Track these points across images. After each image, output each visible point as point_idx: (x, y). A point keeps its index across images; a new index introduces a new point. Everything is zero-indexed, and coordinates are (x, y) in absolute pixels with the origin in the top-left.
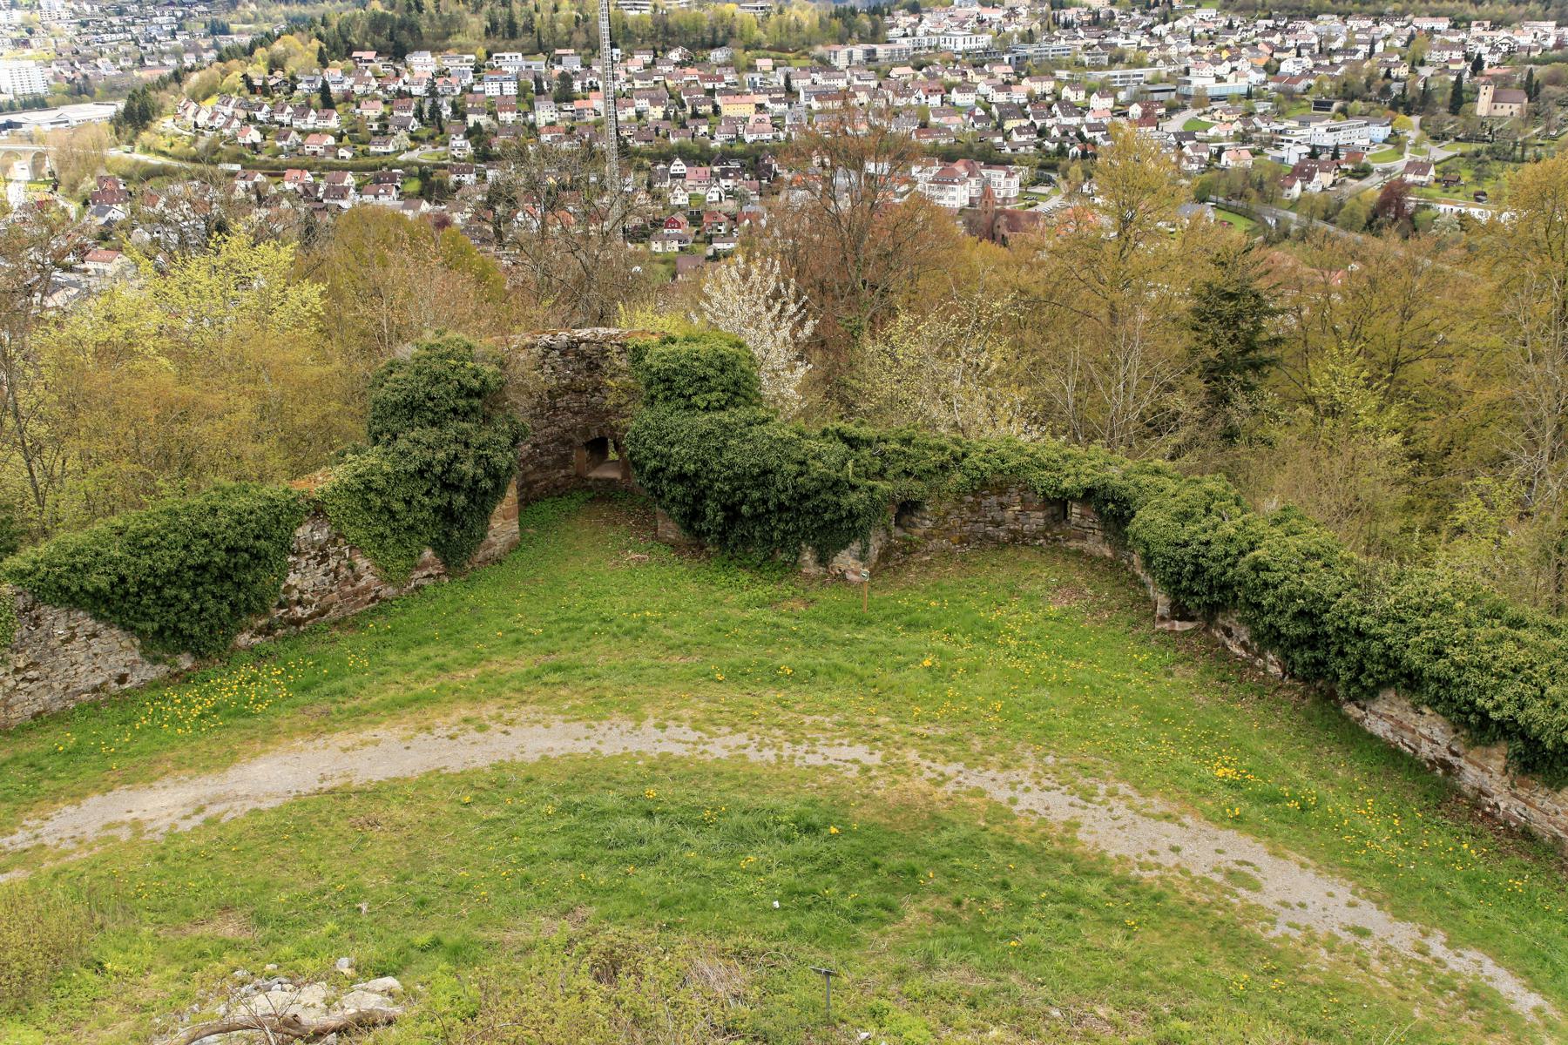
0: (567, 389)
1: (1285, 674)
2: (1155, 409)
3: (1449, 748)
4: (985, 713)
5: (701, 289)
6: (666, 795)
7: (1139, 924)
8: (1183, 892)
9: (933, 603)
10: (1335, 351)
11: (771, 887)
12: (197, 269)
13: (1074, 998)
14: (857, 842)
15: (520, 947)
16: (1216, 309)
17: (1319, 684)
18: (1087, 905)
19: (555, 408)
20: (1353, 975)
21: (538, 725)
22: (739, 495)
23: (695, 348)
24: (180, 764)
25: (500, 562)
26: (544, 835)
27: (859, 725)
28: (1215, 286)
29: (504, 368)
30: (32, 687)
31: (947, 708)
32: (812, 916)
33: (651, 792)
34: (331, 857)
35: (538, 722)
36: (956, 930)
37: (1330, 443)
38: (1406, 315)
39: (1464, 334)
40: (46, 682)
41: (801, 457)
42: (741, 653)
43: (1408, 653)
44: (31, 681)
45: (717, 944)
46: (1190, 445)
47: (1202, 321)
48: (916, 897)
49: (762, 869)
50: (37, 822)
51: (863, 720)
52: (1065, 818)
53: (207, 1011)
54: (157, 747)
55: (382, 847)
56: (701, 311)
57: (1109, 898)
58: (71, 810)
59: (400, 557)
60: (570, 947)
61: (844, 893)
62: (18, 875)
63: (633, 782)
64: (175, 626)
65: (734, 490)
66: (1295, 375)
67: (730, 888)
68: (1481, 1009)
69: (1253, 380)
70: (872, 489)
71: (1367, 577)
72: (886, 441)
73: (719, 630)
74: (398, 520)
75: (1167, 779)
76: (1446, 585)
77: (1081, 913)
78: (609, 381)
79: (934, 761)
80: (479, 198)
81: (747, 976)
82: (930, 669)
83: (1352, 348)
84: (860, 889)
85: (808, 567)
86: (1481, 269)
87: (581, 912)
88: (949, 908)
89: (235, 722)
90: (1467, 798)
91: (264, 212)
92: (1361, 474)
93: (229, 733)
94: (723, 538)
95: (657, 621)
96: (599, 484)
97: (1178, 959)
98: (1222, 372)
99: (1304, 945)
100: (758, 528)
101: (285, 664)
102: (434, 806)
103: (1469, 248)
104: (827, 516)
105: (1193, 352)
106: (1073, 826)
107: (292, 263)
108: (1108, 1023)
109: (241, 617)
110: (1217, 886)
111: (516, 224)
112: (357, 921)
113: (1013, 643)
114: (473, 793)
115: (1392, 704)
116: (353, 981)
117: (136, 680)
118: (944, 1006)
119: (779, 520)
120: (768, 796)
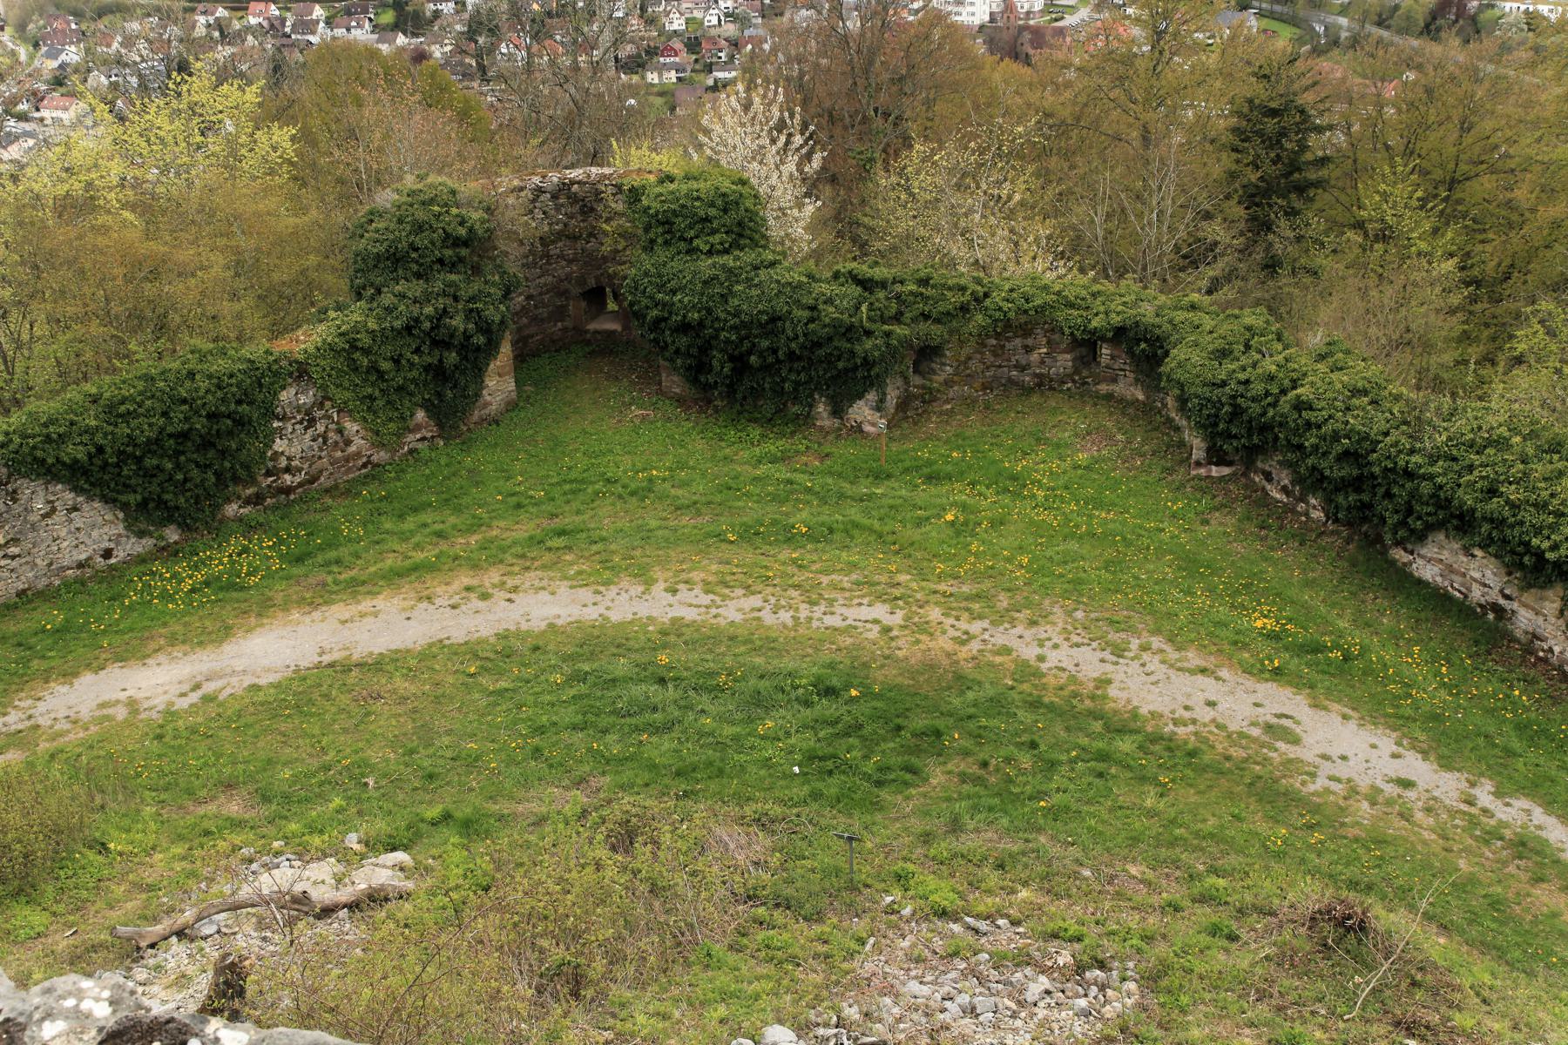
0: (560, 235)
1: (1328, 518)
2: (1191, 240)
3: (1501, 591)
4: (1010, 567)
5: (699, 122)
6: (679, 661)
7: (1173, 781)
8: (1219, 747)
9: (955, 454)
10: (1387, 170)
11: (791, 752)
12: (158, 116)
13: (1106, 858)
14: (879, 704)
15: (532, 819)
16: (1258, 126)
17: (1365, 528)
18: (1119, 763)
19: (548, 256)
20: (1396, 827)
21: (542, 593)
22: (746, 345)
23: (695, 186)
24: (173, 640)
25: (497, 423)
26: (553, 705)
27: (879, 584)
28: (1257, 102)
29: (492, 214)
30: (14, 564)
31: (970, 564)
32: (836, 780)
33: (663, 658)
34: (334, 732)
35: (543, 588)
36: (982, 792)
37: (1380, 270)
38: (1465, 127)
39: (1529, 146)
40: (28, 559)
41: (811, 302)
42: (752, 511)
43: (1460, 492)
44: (13, 558)
45: (734, 810)
46: (1229, 277)
47: (1243, 141)
48: (941, 759)
49: (781, 734)
50: (30, 702)
51: (884, 579)
52: (1095, 675)
53: (215, 889)
54: (149, 623)
55: (387, 720)
56: (699, 147)
57: (1141, 755)
58: (64, 689)
59: (391, 420)
60: (585, 817)
61: (866, 757)
62: (14, 757)
63: (643, 649)
64: (159, 497)
65: (741, 340)
66: (1343, 198)
67: (747, 754)
68: (1528, 859)
69: (1297, 205)
70: (888, 334)
71: (1417, 413)
72: (902, 282)
73: (730, 489)
74: (387, 381)
75: (1203, 632)
76: (1502, 419)
77: (1113, 771)
78: (604, 226)
79: (958, 619)
80: (458, 27)
81: (768, 843)
82: (952, 523)
83: (1406, 165)
84: (883, 752)
85: (822, 419)
86: (1549, 73)
87: (594, 782)
88: (975, 770)
89: (228, 595)
90: (1519, 642)
91: (228, 50)
92: (1413, 303)
93: (222, 608)
94: (731, 391)
95: (664, 480)
96: (599, 337)
97: (1214, 815)
98: (1263, 197)
99: (1345, 798)
100: (768, 379)
101: (277, 535)
102: (438, 678)
103: (1536, 49)
104: (841, 365)
105: (1233, 176)
106: (1104, 682)
107: (260, 105)
108: (1141, 881)
109: (227, 486)
110: (1255, 740)
111: (499, 57)
112: (365, 796)
113: (1041, 494)
114: (478, 663)
115: (1441, 547)
116: (363, 857)
117: (122, 554)
118: (971, 868)
119: (790, 370)
120: (786, 660)
